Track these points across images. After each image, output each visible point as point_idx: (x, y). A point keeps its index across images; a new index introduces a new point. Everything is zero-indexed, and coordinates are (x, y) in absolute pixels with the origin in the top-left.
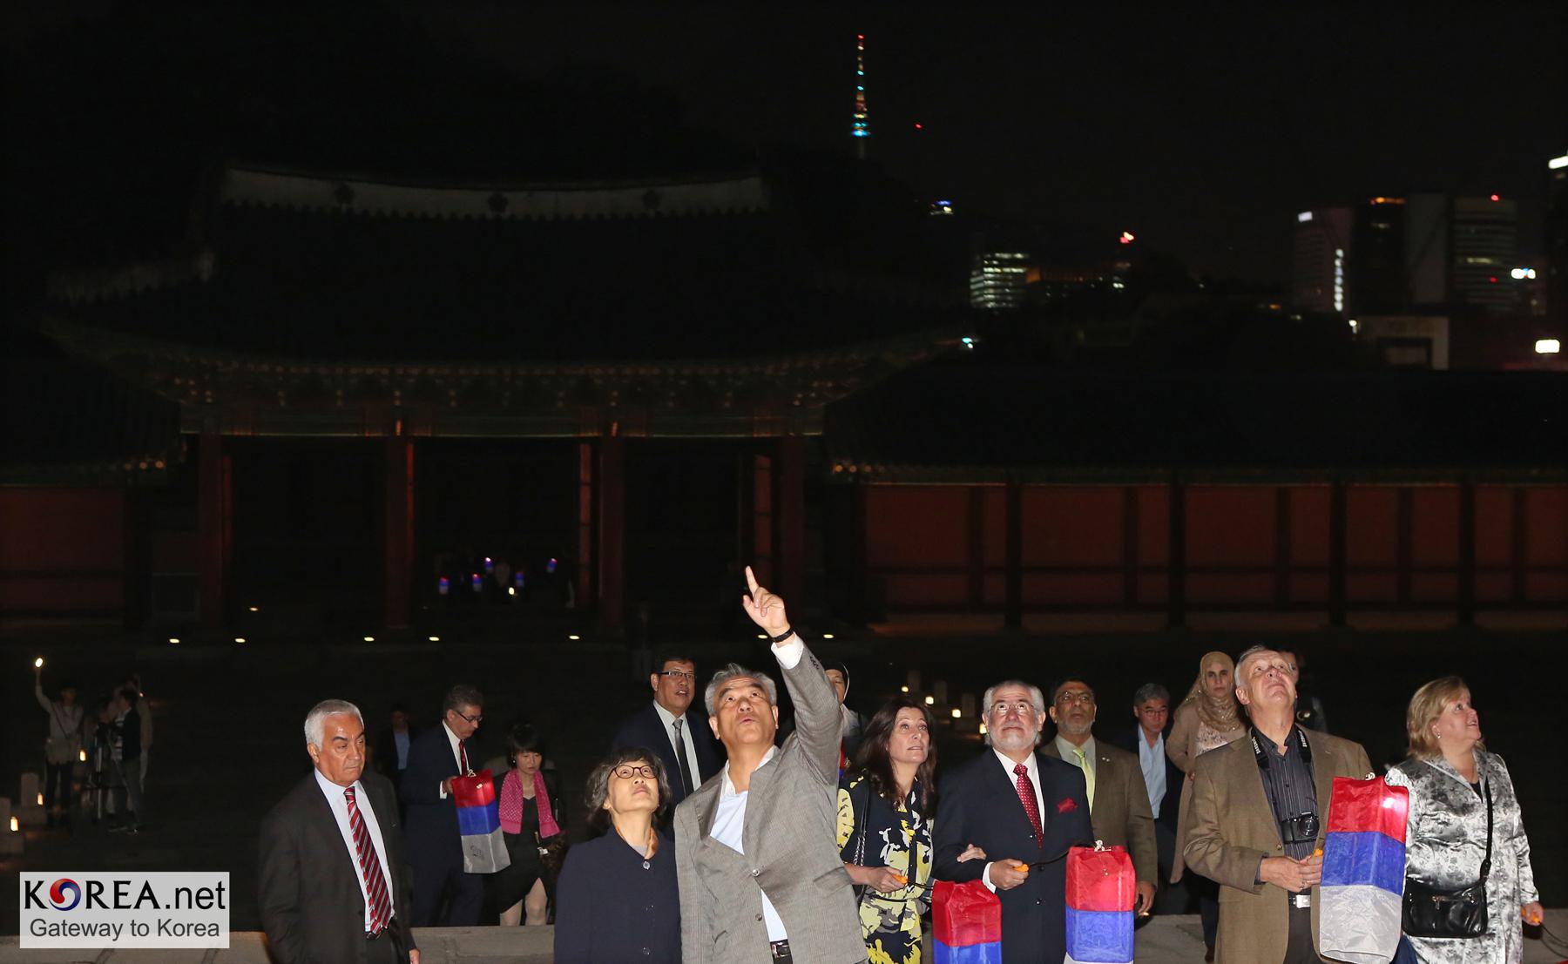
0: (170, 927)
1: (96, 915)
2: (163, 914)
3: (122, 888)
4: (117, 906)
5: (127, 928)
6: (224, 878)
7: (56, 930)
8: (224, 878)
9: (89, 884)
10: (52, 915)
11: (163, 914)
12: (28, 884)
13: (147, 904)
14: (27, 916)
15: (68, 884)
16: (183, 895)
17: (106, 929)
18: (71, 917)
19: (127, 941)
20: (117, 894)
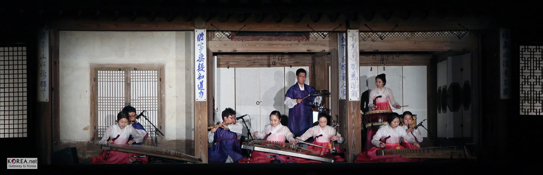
0: (29, 166)
1: (18, 164)
2: (28, 164)
3: (22, 160)
4: (21, 163)
5: (22, 166)
6: (37, 159)
7: (12, 166)
8: (37, 159)
9: (17, 160)
10: (12, 164)
11: (28, 164)
12: (8, 160)
13: (25, 163)
14: (8, 164)
15: (14, 160)
16: (31, 161)
17: (19, 166)
18: (14, 164)
19: (23, 168)
20: (21, 161)
